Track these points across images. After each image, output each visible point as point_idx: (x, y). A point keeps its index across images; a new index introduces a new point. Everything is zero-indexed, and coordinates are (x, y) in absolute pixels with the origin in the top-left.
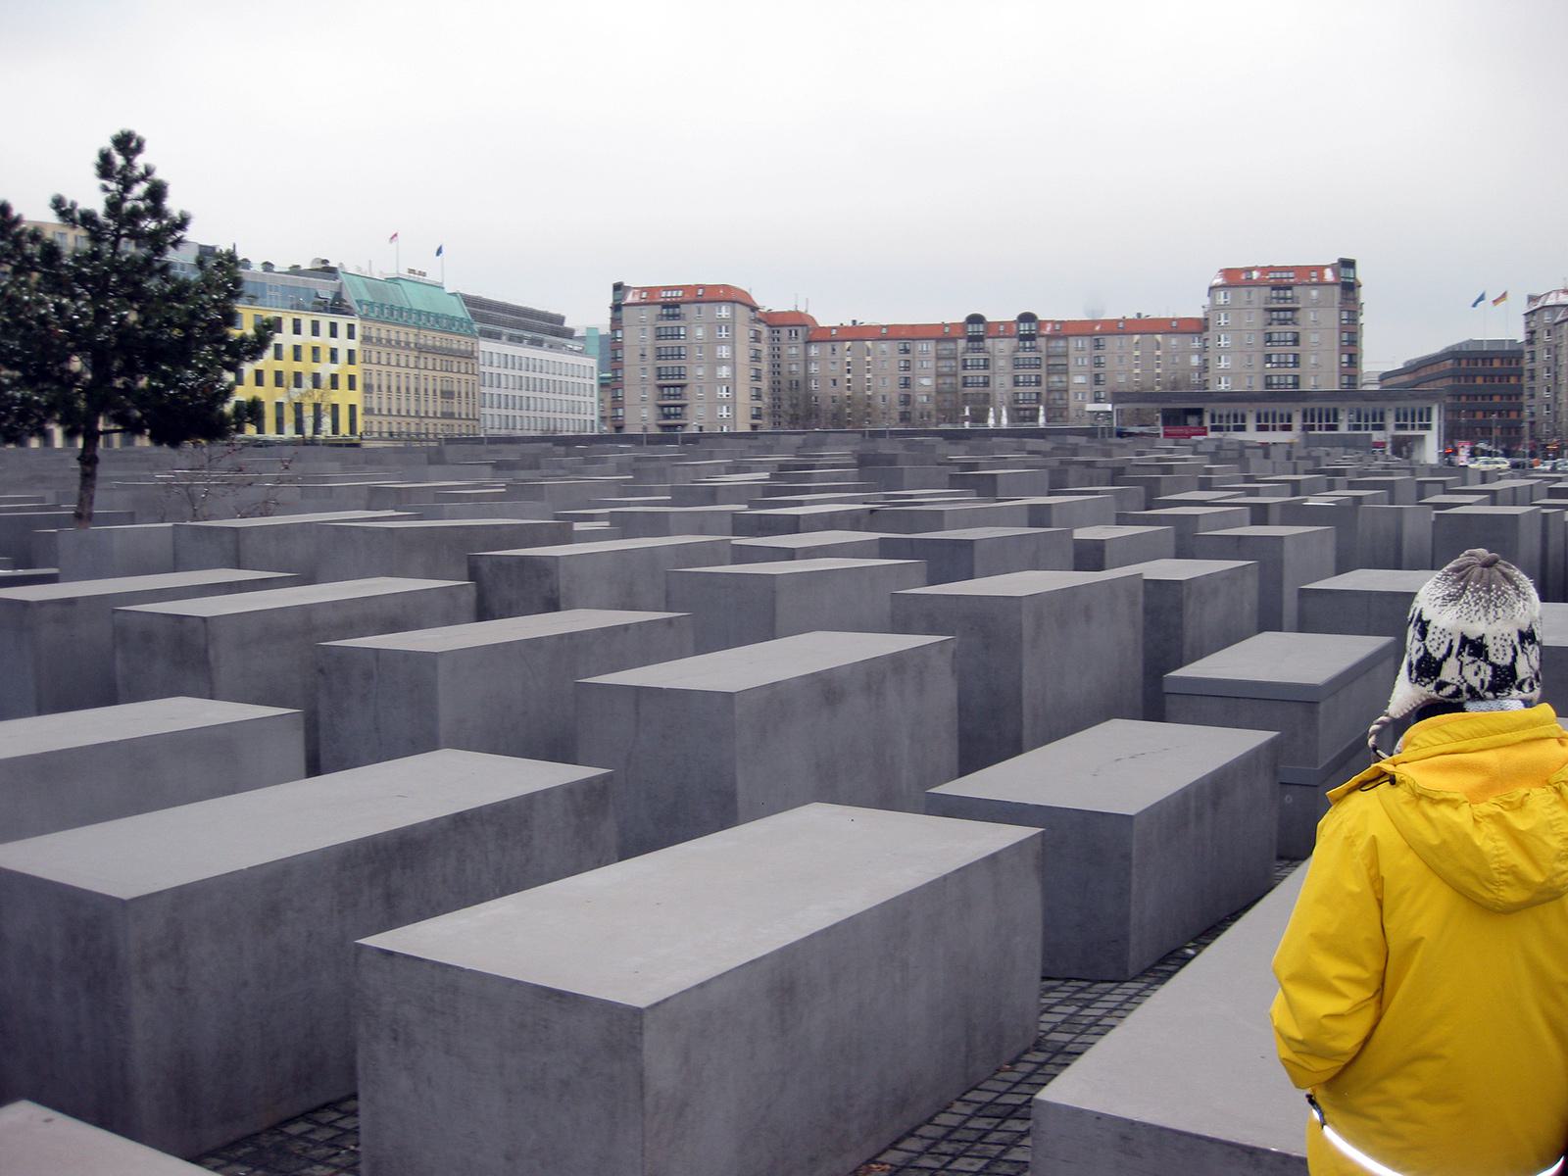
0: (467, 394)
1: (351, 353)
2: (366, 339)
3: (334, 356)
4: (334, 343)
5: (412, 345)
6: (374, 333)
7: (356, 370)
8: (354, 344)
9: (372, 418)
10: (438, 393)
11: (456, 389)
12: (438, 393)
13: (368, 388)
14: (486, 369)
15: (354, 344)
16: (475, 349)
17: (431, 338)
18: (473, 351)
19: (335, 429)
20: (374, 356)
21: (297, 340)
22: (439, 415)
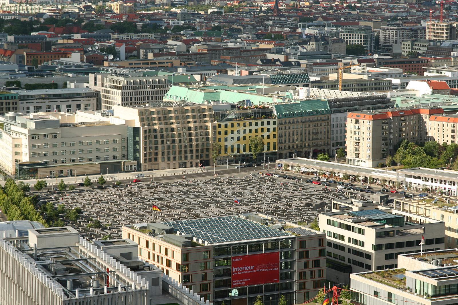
0: (325, 132)
1: (274, 129)
2: (280, 124)
3: (268, 130)
4: (268, 127)
5: (300, 122)
6: (283, 122)
7: (276, 133)
8: (276, 126)
9: (282, 145)
10: (311, 134)
11: (319, 131)
12: (311, 134)
13: (280, 137)
14: (335, 123)
15: (276, 126)
16: (329, 117)
17: (307, 118)
18: (328, 119)
19: (268, 149)
20: (283, 128)
21: (256, 127)
22: (311, 140)
